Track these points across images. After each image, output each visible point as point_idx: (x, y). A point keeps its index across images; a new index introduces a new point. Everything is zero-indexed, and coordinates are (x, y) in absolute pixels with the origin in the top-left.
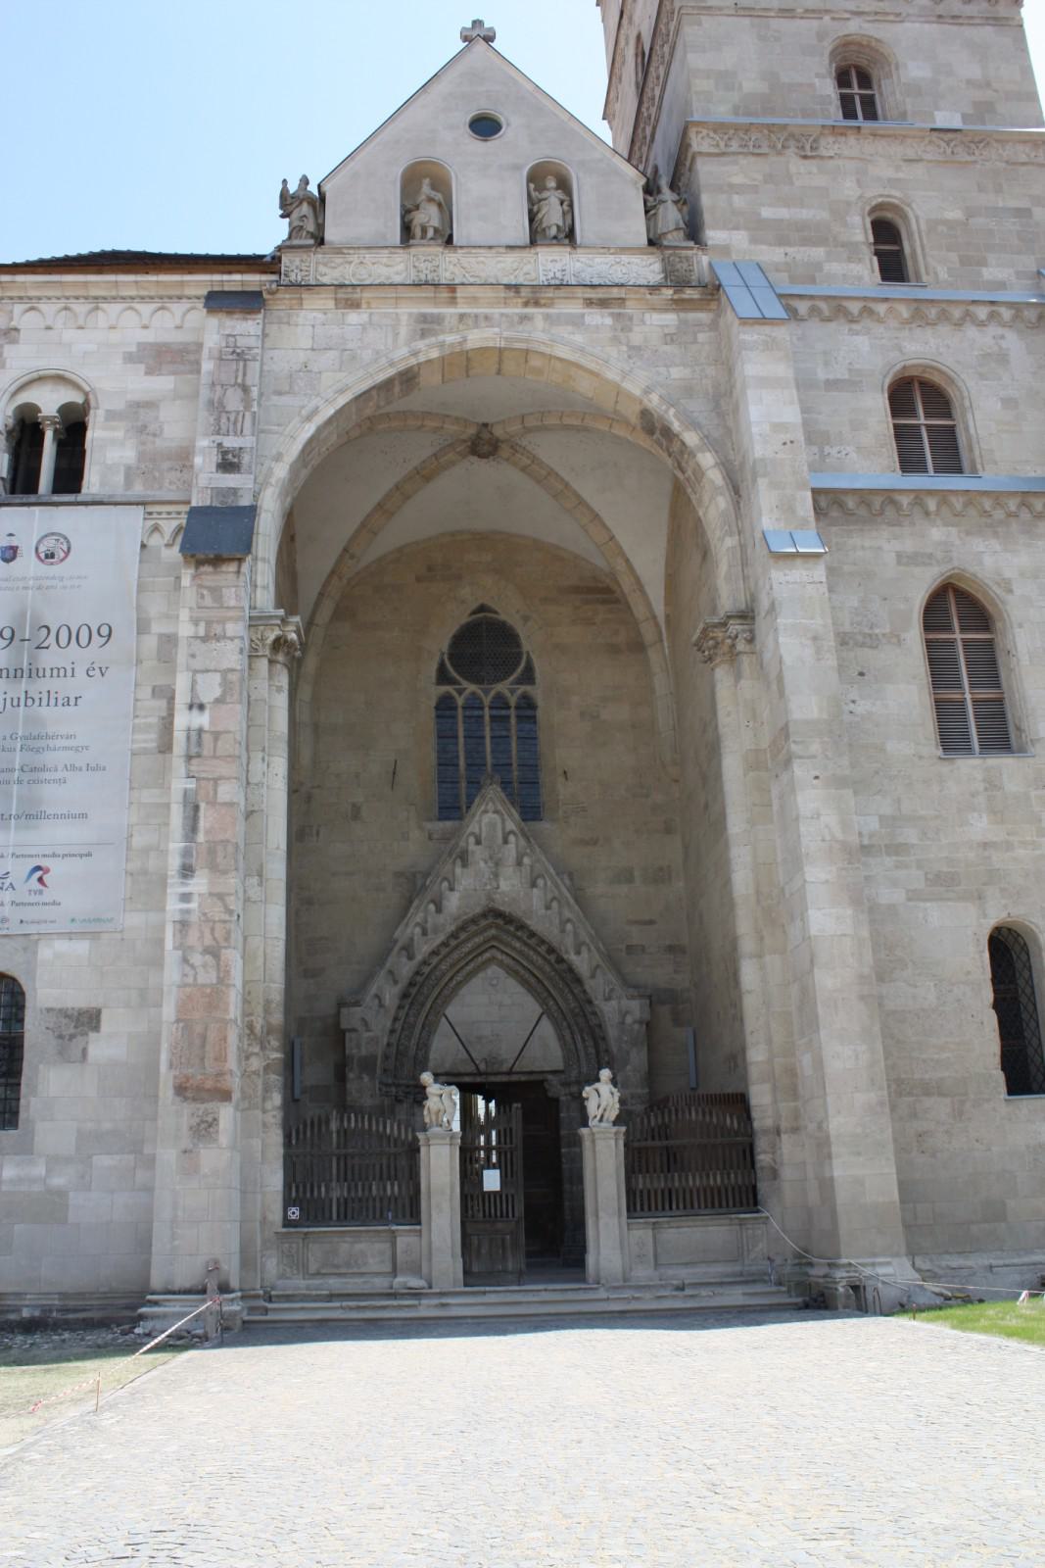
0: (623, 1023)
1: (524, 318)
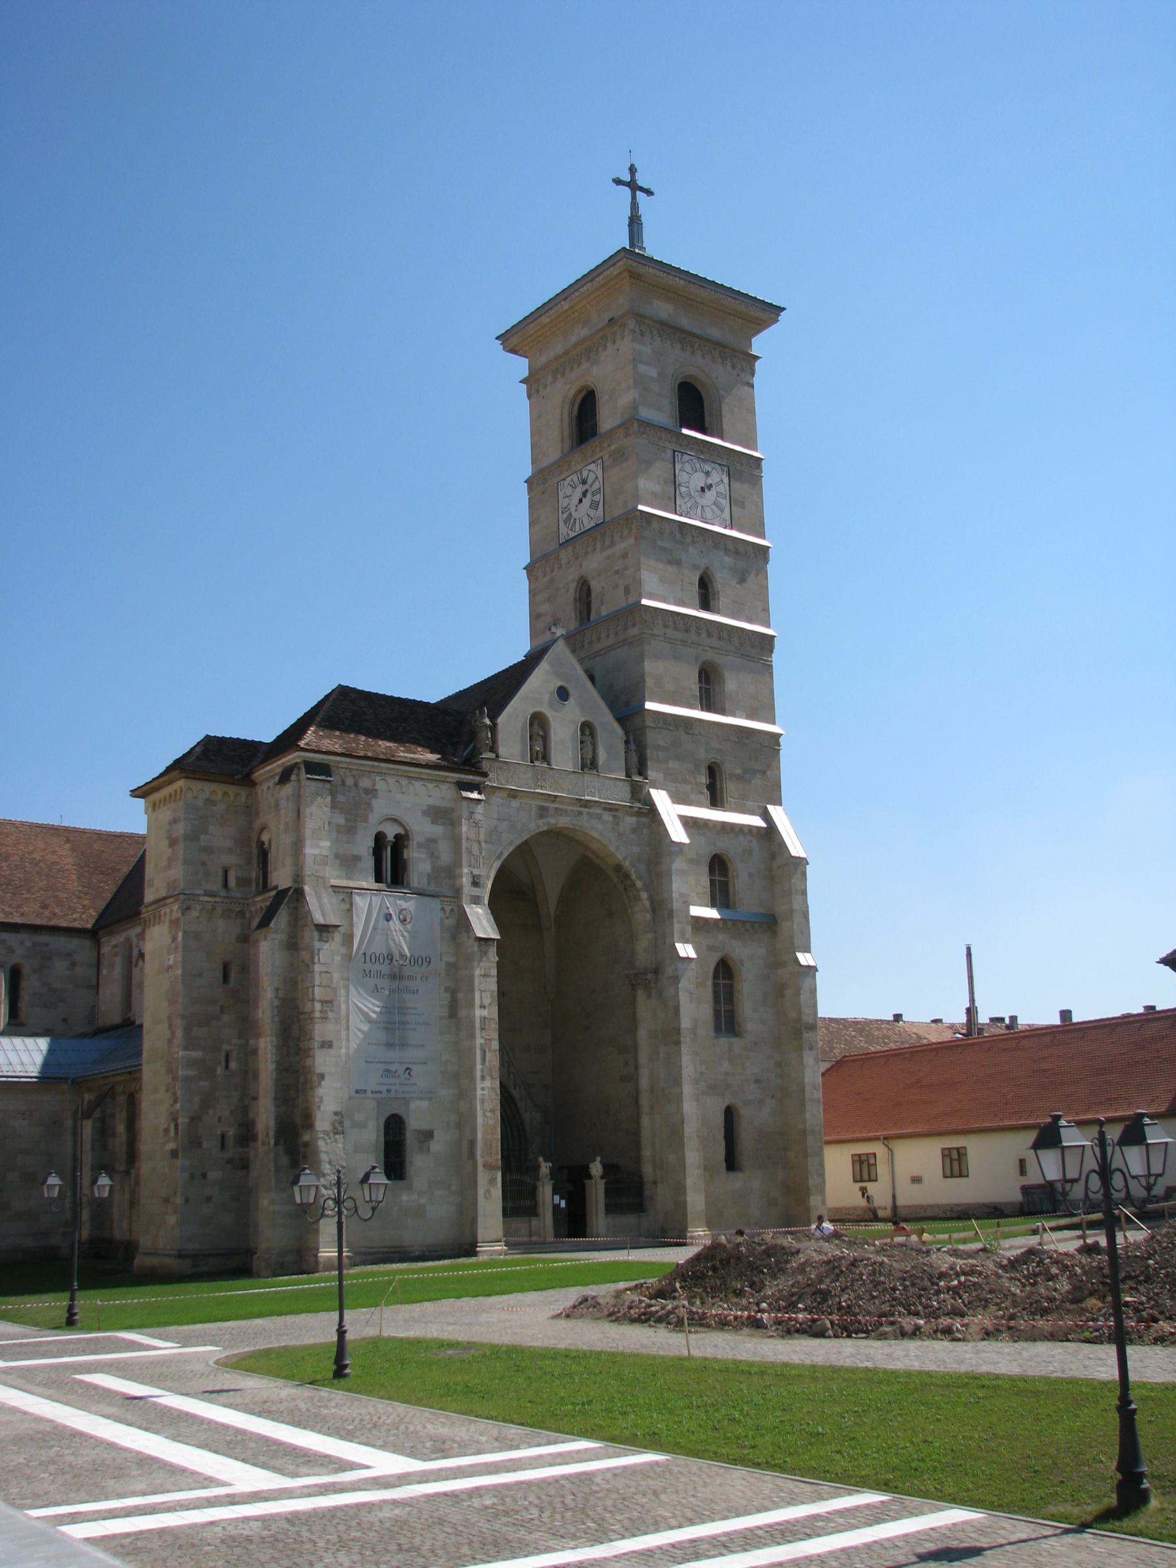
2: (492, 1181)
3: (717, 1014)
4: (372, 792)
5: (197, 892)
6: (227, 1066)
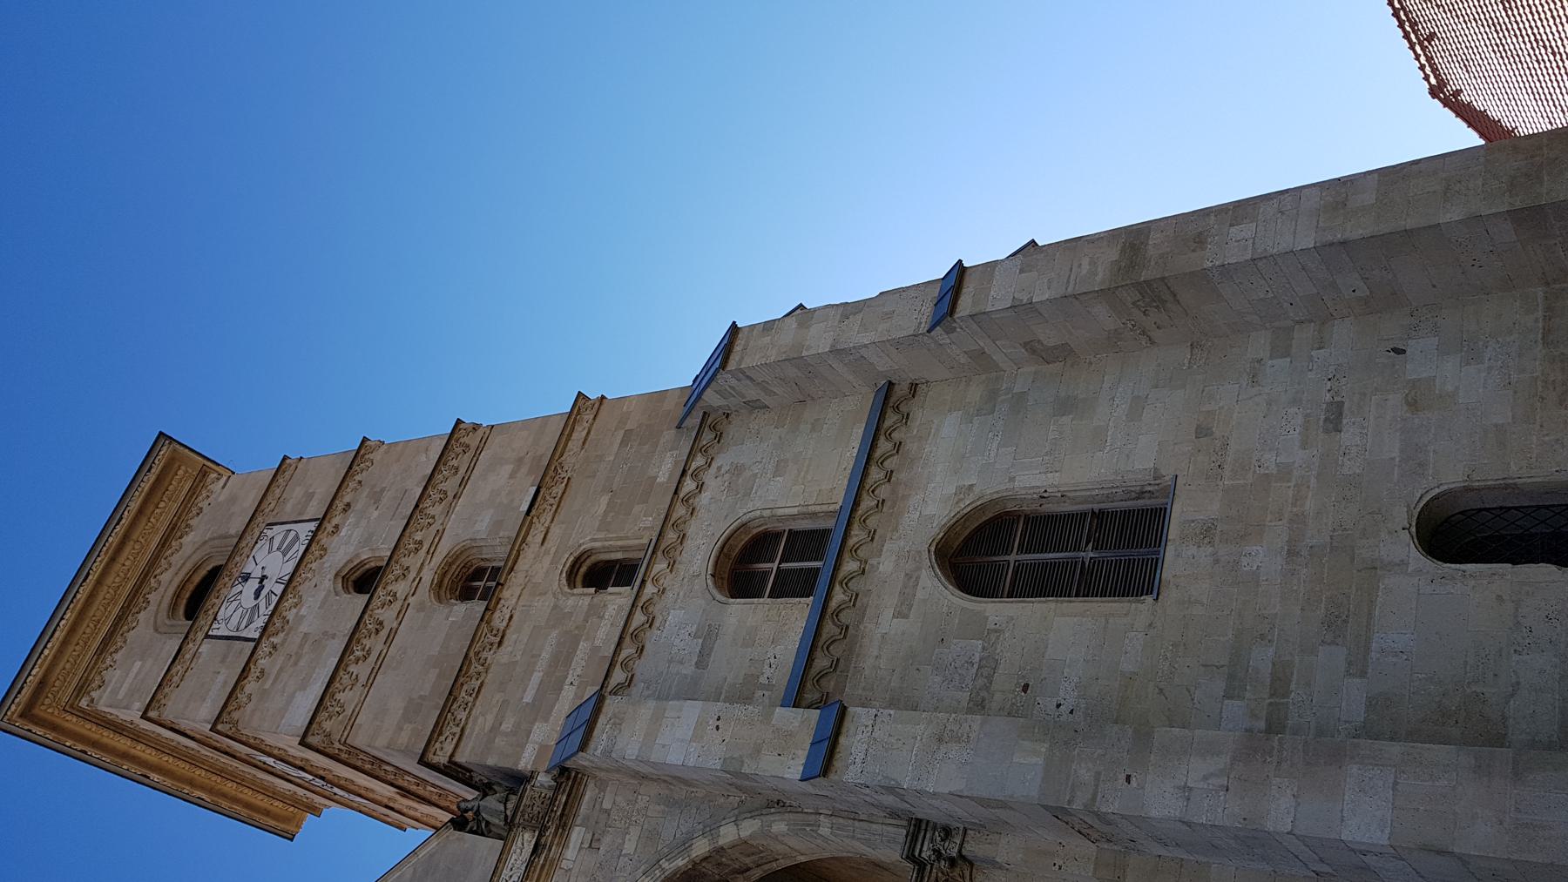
3: (1087, 584)
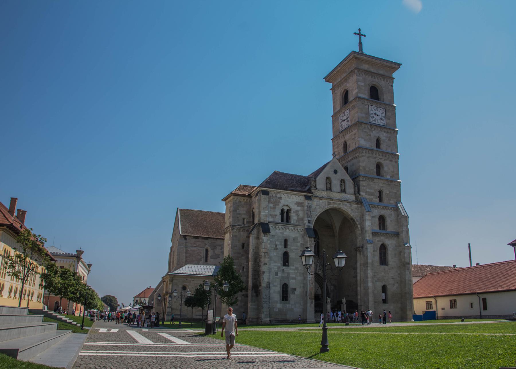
0: (331, 289)
1: (340, 204)
2: (312, 303)
4: (281, 198)
5: (236, 225)
6: (243, 270)
